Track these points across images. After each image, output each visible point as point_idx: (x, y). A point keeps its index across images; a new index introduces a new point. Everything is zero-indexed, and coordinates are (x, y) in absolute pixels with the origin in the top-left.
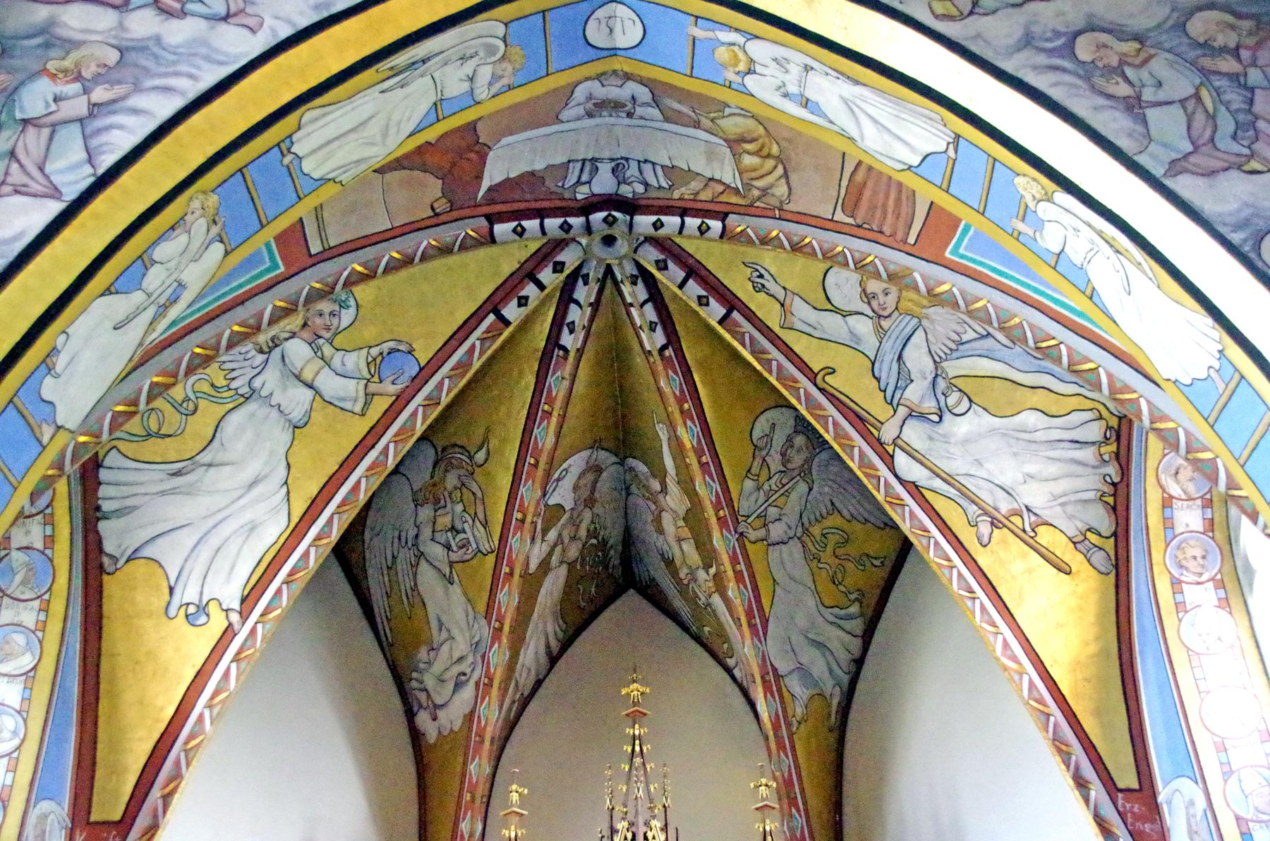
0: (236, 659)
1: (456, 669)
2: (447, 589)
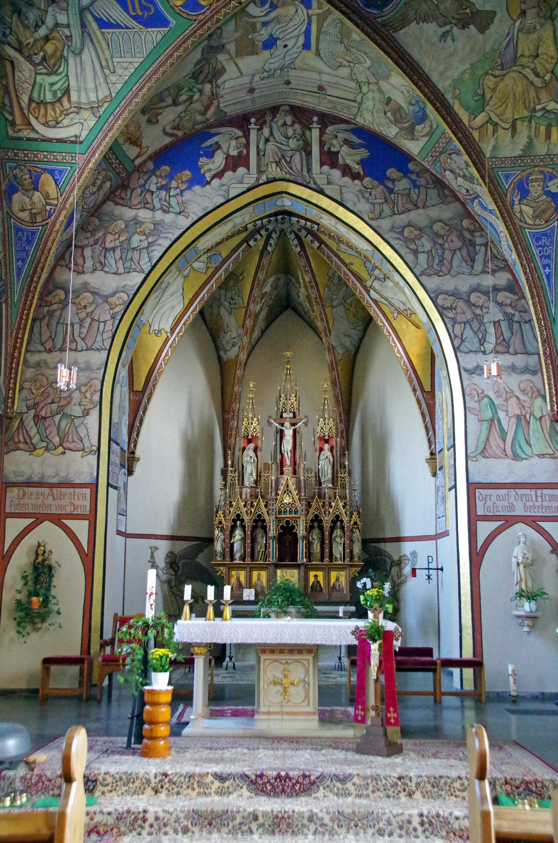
0: (170, 347)
1: (233, 341)
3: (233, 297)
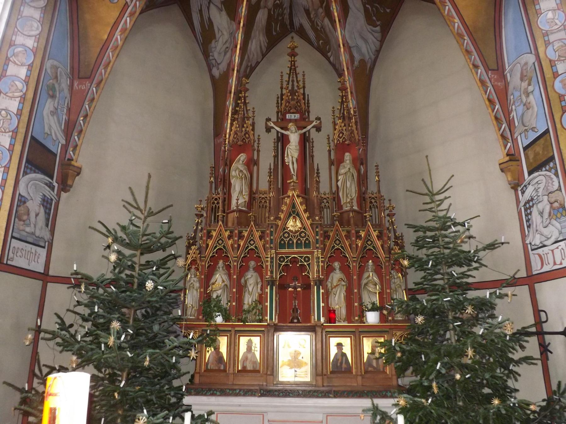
2: (220, 13)
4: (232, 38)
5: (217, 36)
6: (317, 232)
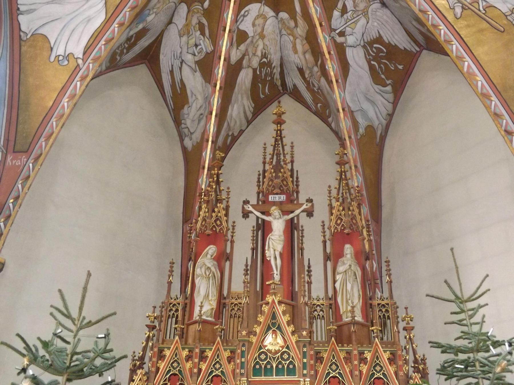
2: (194, 75)
3: (198, 43)
4: (207, 103)
5: (190, 100)
6: (304, 353)
